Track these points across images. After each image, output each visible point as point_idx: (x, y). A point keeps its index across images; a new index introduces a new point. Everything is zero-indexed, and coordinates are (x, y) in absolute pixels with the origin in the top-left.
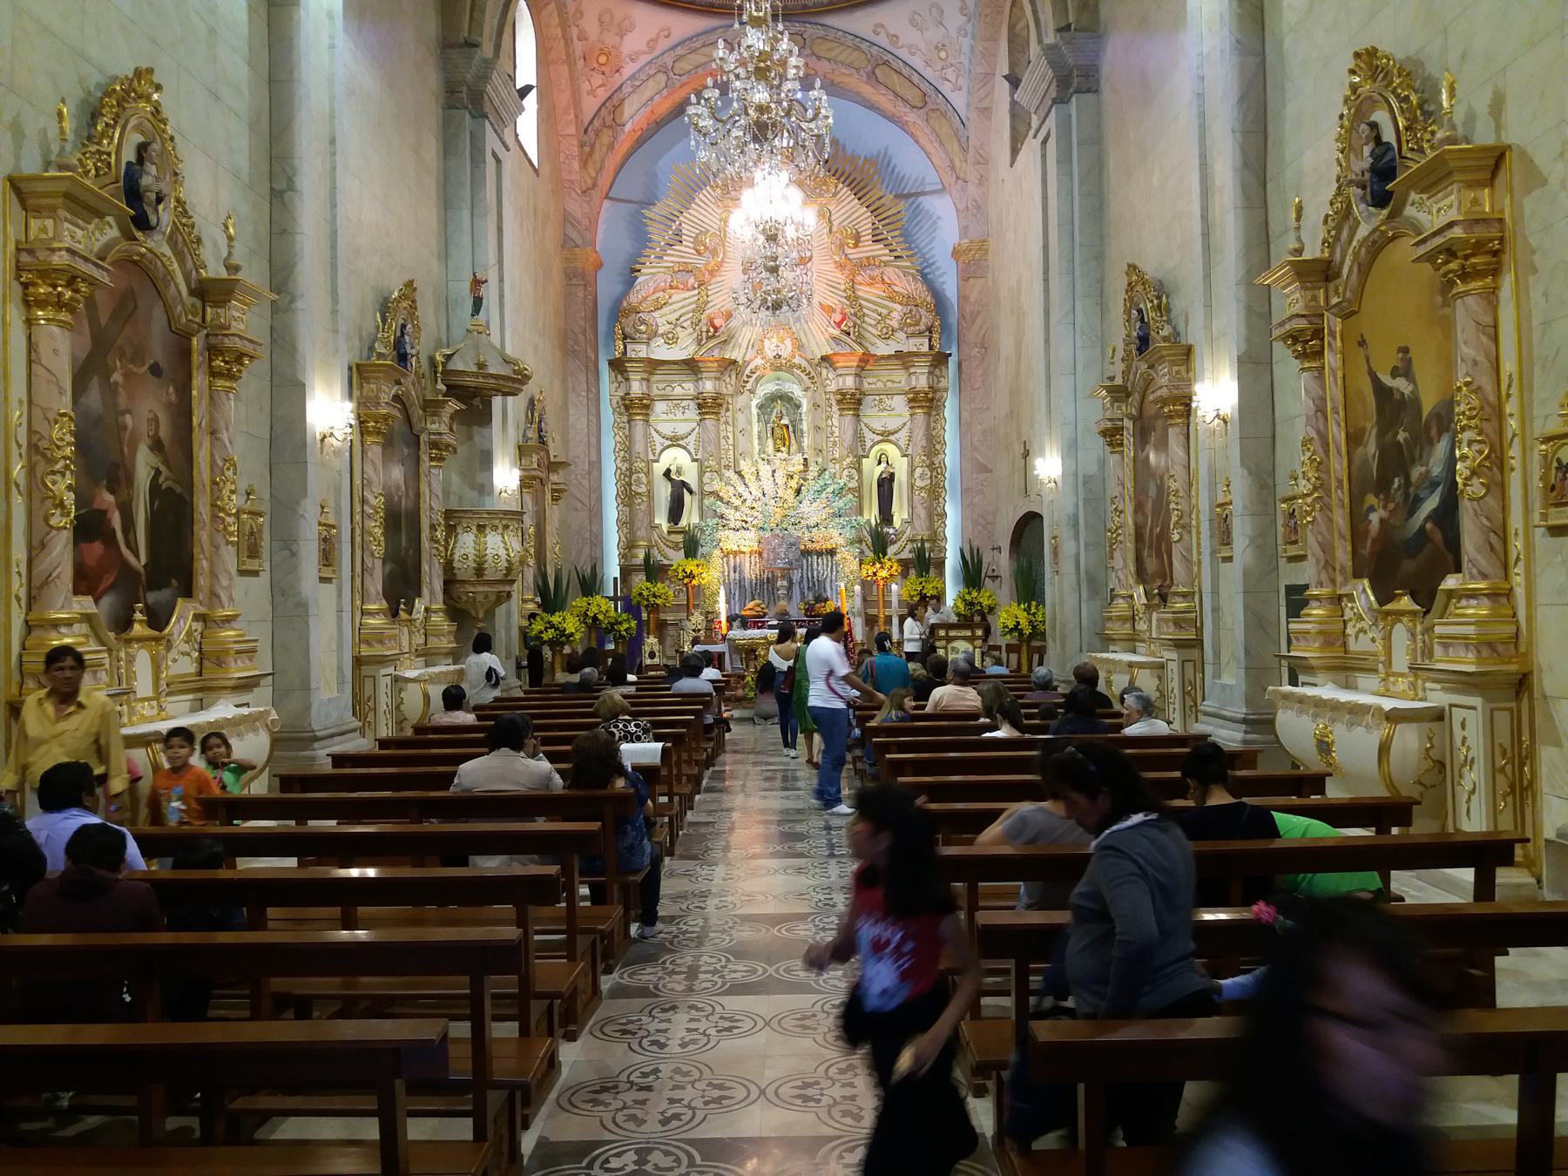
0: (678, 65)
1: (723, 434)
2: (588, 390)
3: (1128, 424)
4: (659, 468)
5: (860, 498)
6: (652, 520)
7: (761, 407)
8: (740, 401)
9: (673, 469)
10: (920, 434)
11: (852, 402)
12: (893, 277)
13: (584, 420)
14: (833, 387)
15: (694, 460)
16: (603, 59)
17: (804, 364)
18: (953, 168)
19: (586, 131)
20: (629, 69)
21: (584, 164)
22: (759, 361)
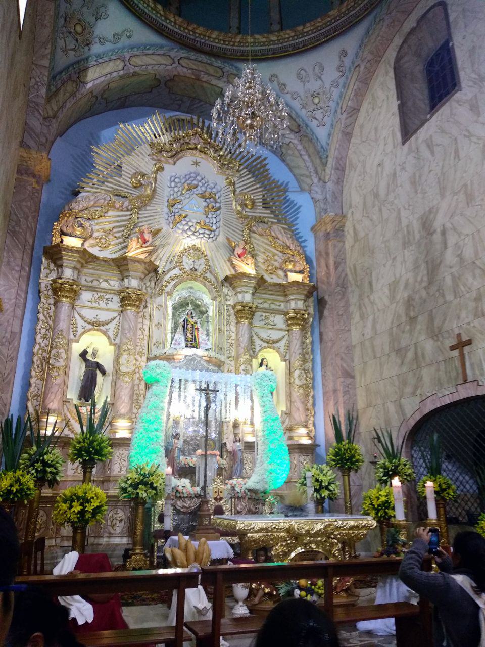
0: (133, 59)
1: (140, 325)
2: (22, 268)
4: (77, 348)
6: (64, 396)
8: (158, 301)
9: (90, 351)
12: (278, 233)
13: (13, 291)
15: (111, 344)
16: (79, 29)
17: (213, 280)
18: (317, 173)
19: (54, 78)
20: (96, 48)
21: (49, 99)
22: (177, 271)
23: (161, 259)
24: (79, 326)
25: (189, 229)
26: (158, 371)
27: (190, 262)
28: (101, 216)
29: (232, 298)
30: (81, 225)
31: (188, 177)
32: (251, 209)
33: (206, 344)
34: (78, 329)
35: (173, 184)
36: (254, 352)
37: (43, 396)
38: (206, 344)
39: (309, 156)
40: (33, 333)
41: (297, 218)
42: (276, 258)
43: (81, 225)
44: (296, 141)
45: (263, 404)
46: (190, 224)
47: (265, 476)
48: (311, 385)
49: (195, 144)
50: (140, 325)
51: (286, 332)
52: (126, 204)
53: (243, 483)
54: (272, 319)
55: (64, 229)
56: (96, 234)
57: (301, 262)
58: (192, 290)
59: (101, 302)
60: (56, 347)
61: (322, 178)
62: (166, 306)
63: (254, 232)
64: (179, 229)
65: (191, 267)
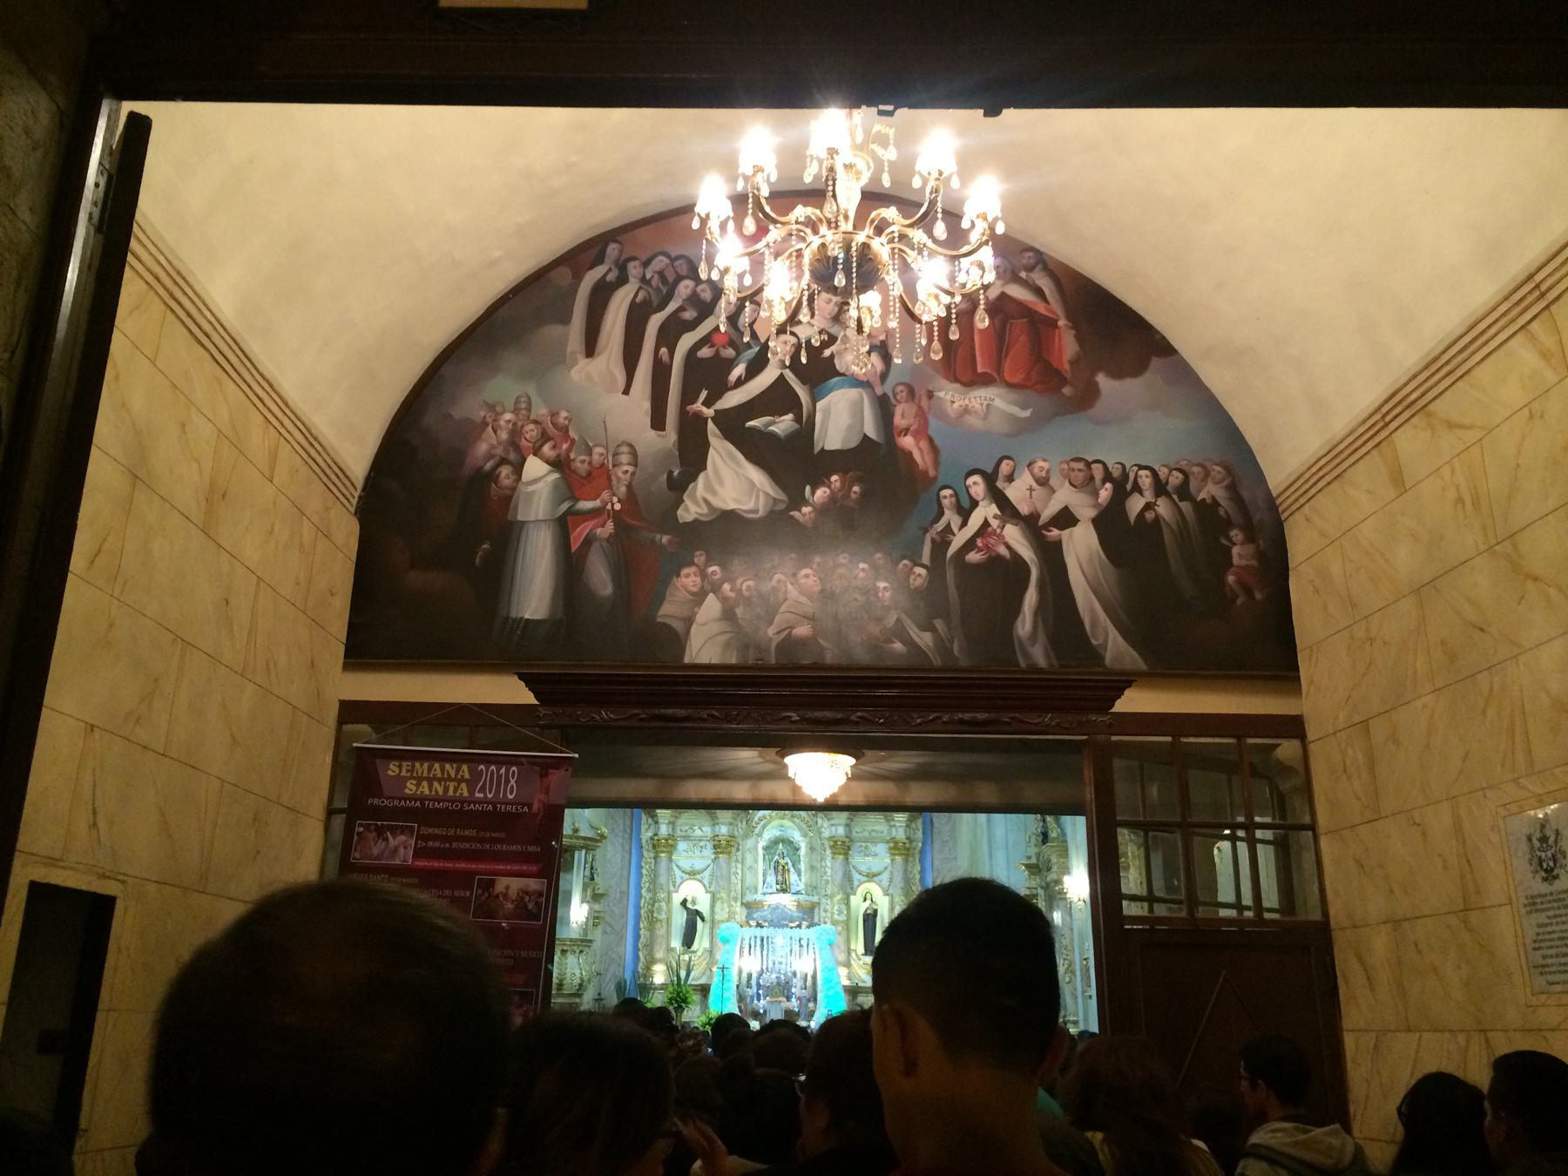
3: (1041, 892)
5: (848, 930)
7: (766, 848)
8: (750, 842)
11: (843, 848)
13: (619, 856)
14: (826, 834)
37: (650, 946)
40: (639, 887)
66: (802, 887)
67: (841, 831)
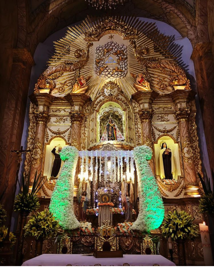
1: (83, 132)
7: (103, 120)
8: (92, 116)
9: (57, 149)
10: (184, 131)
11: (148, 116)
14: (137, 110)
18: (189, 23)
22: (101, 98)
23: (93, 93)
24: (49, 136)
25: (109, 74)
26: (67, 153)
27: (108, 91)
28: (59, 76)
29: (138, 108)
30: (49, 83)
31: (106, 46)
32: (146, 54)
33: (121, 137)
34: (49, 138)
35: (98, 51)
36: (155, 139)
38: (121, 137)
39: (183, 14)
41: (182, 54)
42: (166, 79)
43: (49, 83)
44: (173, 9)
45: (141, 168)
46: (109, 71)
47: (144, 220)
48: (199, 157)
49: (110, 26)
50: (83, 132)
51: (176, 125)
52: (72, 67)
53: (130, 225)
54: (166, 117)
55: (40, 86)
56: (57, 87)
57: (183, 79)
58: (111, 107)
59: (61, 122)
60: (36, 148)
61: (194, 25)
62: (96, 118)
63: (149, 67)
64: (103, 74)
65: (109, 94)
66: (124, 138)
67: (146, 106)
